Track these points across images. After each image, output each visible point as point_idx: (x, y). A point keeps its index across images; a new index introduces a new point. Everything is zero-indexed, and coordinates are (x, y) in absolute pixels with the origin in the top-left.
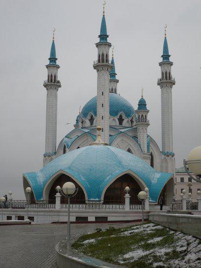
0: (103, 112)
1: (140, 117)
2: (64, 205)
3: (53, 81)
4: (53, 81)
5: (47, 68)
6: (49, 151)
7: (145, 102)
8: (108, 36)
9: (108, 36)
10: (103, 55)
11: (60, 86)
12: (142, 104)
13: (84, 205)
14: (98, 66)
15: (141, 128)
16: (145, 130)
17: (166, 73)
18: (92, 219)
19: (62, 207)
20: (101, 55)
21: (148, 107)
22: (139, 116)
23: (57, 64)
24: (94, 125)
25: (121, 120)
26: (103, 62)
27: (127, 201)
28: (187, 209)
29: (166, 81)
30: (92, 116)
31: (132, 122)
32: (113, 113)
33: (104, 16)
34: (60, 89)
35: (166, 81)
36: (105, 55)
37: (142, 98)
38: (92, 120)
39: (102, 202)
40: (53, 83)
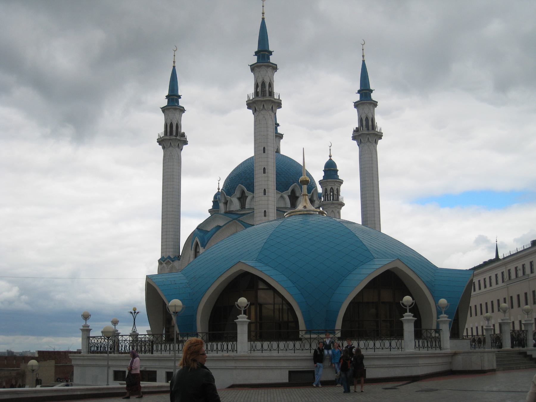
0: (266, 182)
1: (329, 192)
3: (174, 133)
4: (174, 133)
5: (163, 111)
6: (168, 254)
9: (271, 53)
11: (186, 143)
12: (331, 170)
16: (337, 214)
19: (252, 349)
20: (260, 85)
21: (341, 175)
22: (326, 189)
23: (180, 104)
26: (264, 95)
27: (409, 329)
28: (512, 347)
29: (367, 134)
30: (243, 192)
32: (281, 186)
33: (263, 19)
34: (185, 147)
37: (330, 159)
38: (242, 199)
39: (339, 335)
40: (173, 139)
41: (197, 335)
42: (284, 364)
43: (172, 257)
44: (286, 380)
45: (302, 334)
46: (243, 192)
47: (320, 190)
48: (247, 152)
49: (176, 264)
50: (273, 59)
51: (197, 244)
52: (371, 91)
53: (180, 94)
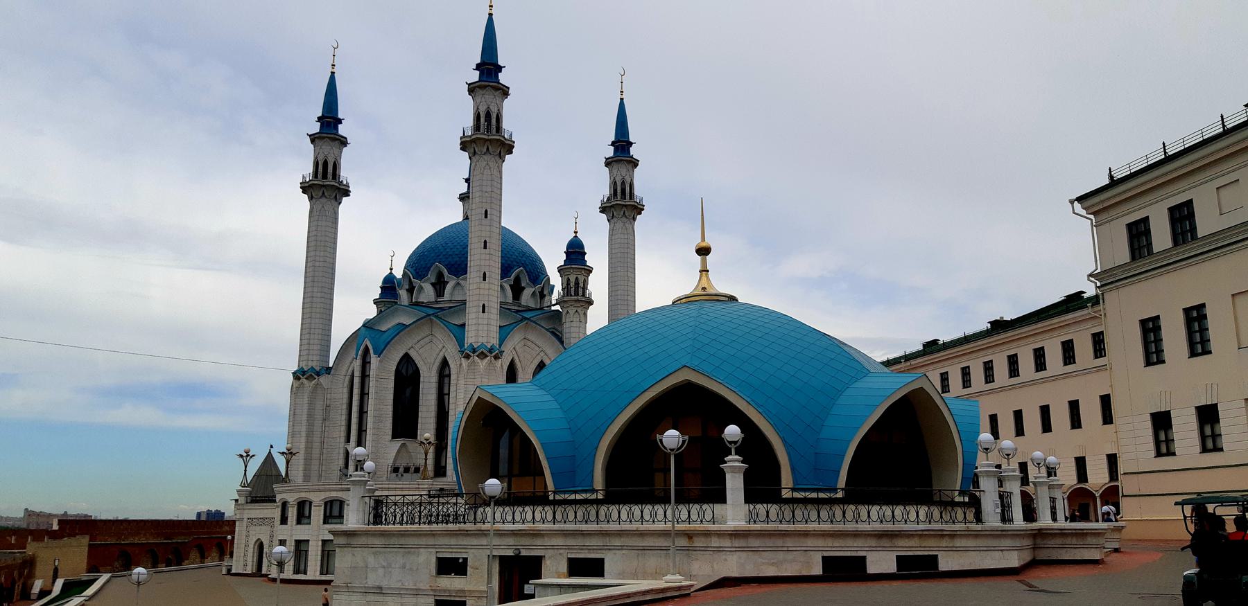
0: (484, 262)
2: (761, 508)
3: (330, 176)
5: (312, 141)
6: (310, 364)
7: (582, 247)
8: (500, 69)
9: (500, 69)
10: (488, 115)
11: (346, 193)
12: (575, 252)
13: (774, 509)
14: (474, 141)
15: (572, 312)
17: (623, 183)
18: (881, 561)
19: (751, 518)
21: (590, 260)
24: (447, 297)
25: (517, 290)
29: (622, 206)
30: (440, 275)
31: (542, 296)
35: (622, 206)
36: (494, 116)
38: (439, 286)
40: (325, 187)
41: (594, 491)
42: (820, 543)
43: (318, 369)
44: (817, 570)
45: (786, 494)
46: (440, 275)
47: (556, 280)
48: (453, 214)
49: (324, 380)
50: (503, 78)
51: (367, 350)
52: (631, 144)
53: (340, 116)
